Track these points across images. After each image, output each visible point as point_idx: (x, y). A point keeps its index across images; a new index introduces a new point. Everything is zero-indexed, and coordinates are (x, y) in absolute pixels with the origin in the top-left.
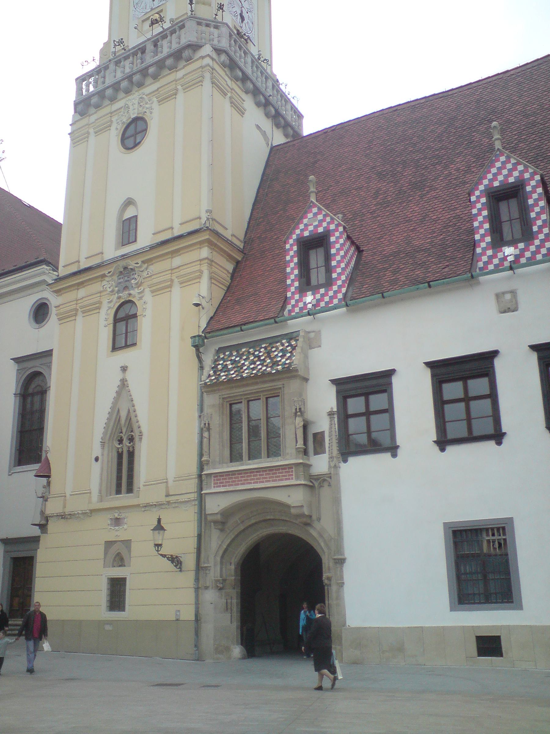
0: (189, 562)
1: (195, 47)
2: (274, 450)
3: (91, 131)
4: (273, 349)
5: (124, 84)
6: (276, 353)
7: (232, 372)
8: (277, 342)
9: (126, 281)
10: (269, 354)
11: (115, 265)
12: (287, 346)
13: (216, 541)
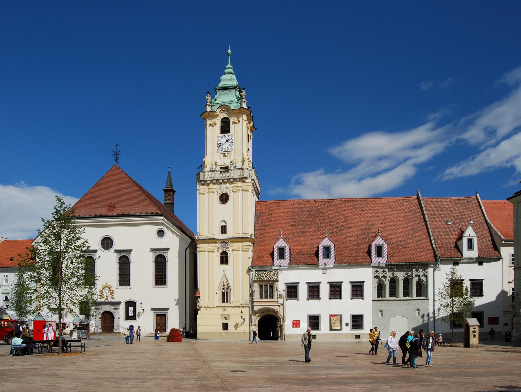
0: (247, 320)
1: (247, 178)
2: (271, 297)
3: (207, 191)
5: (221, 181)
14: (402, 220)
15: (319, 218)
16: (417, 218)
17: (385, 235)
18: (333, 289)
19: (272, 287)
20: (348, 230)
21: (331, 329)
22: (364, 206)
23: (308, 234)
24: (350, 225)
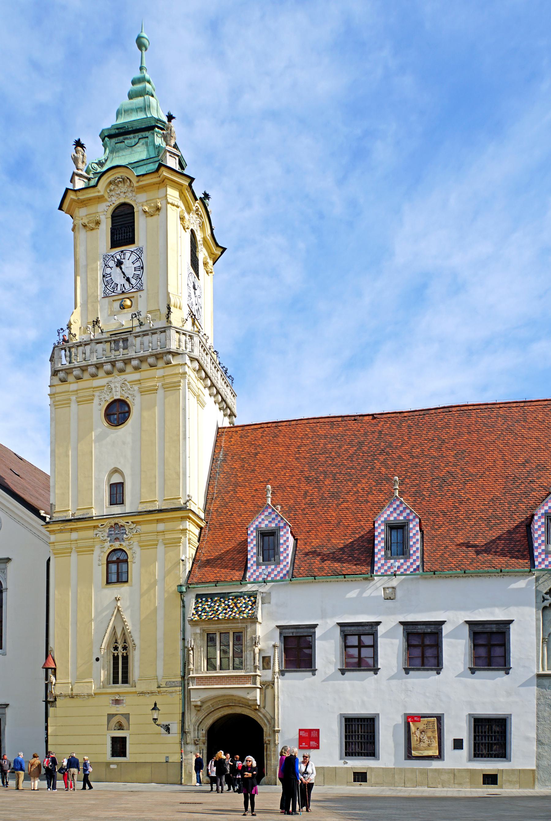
4: (239, 602)
6: (241, 604)
7: (210, 614)
8: (241, 597)
9: (117, 534)
10: (235, 604)
11: (108, 521)
12: (248, 601)
13: (192, 718)
15: (382, 458)
18: (415, 641)
19: (238, 638)
21: (409, 756)
23: (349, 498)
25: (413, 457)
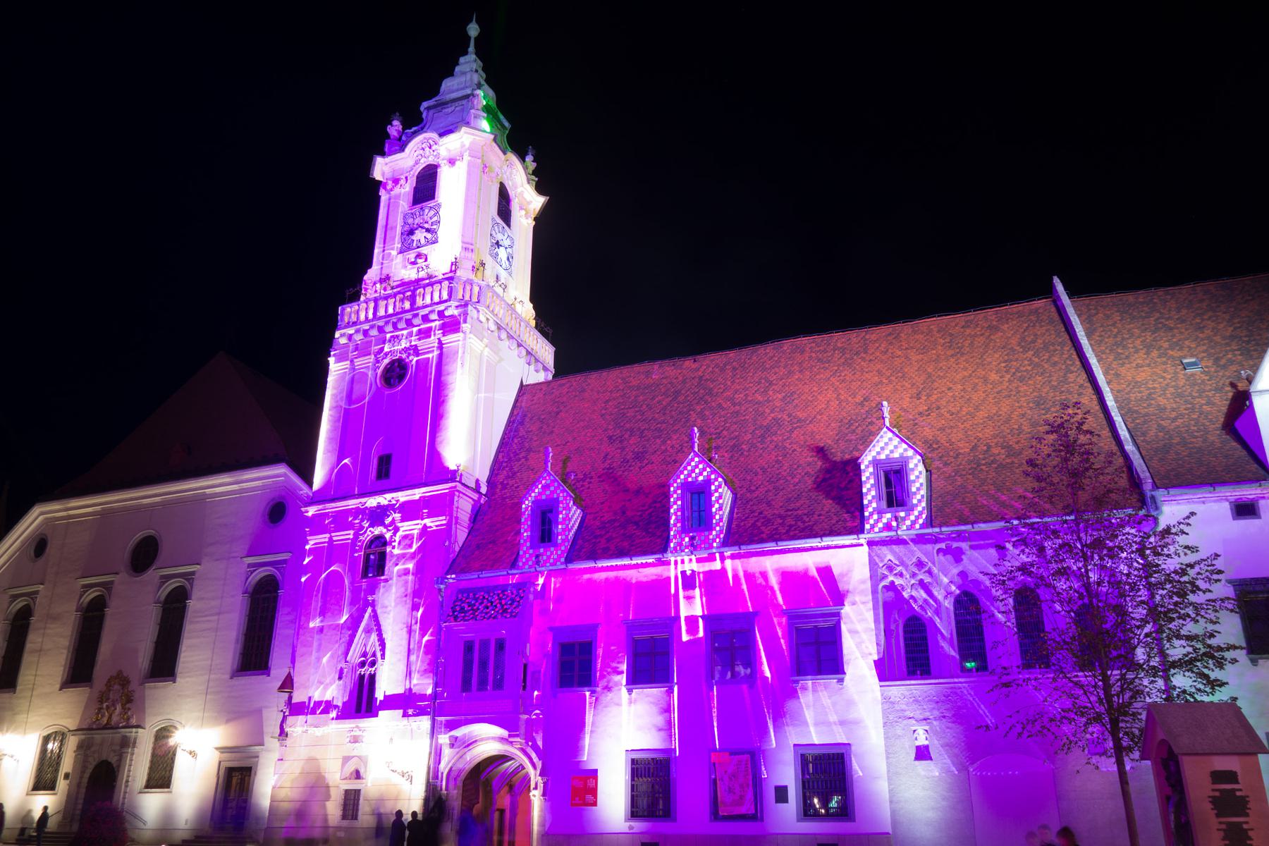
14: (994, 377)
16: (1055, 364)
17: (928, 433)
20: (792, 431)
22: (857, 353)
24: (801, 415)
25: (734, 404)
